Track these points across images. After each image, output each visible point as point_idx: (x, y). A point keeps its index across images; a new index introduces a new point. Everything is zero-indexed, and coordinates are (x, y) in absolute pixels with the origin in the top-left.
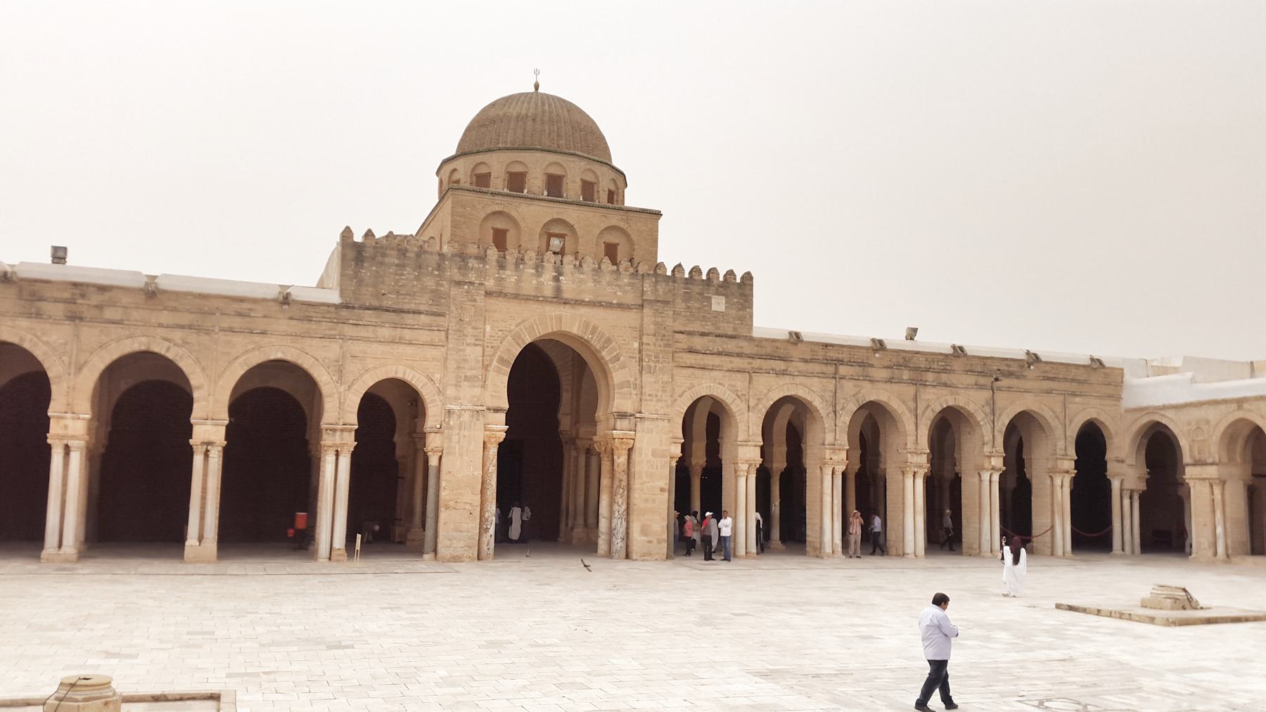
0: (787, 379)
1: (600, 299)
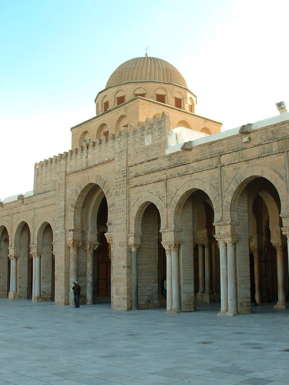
0: (187, 178)
1: (101, 160)
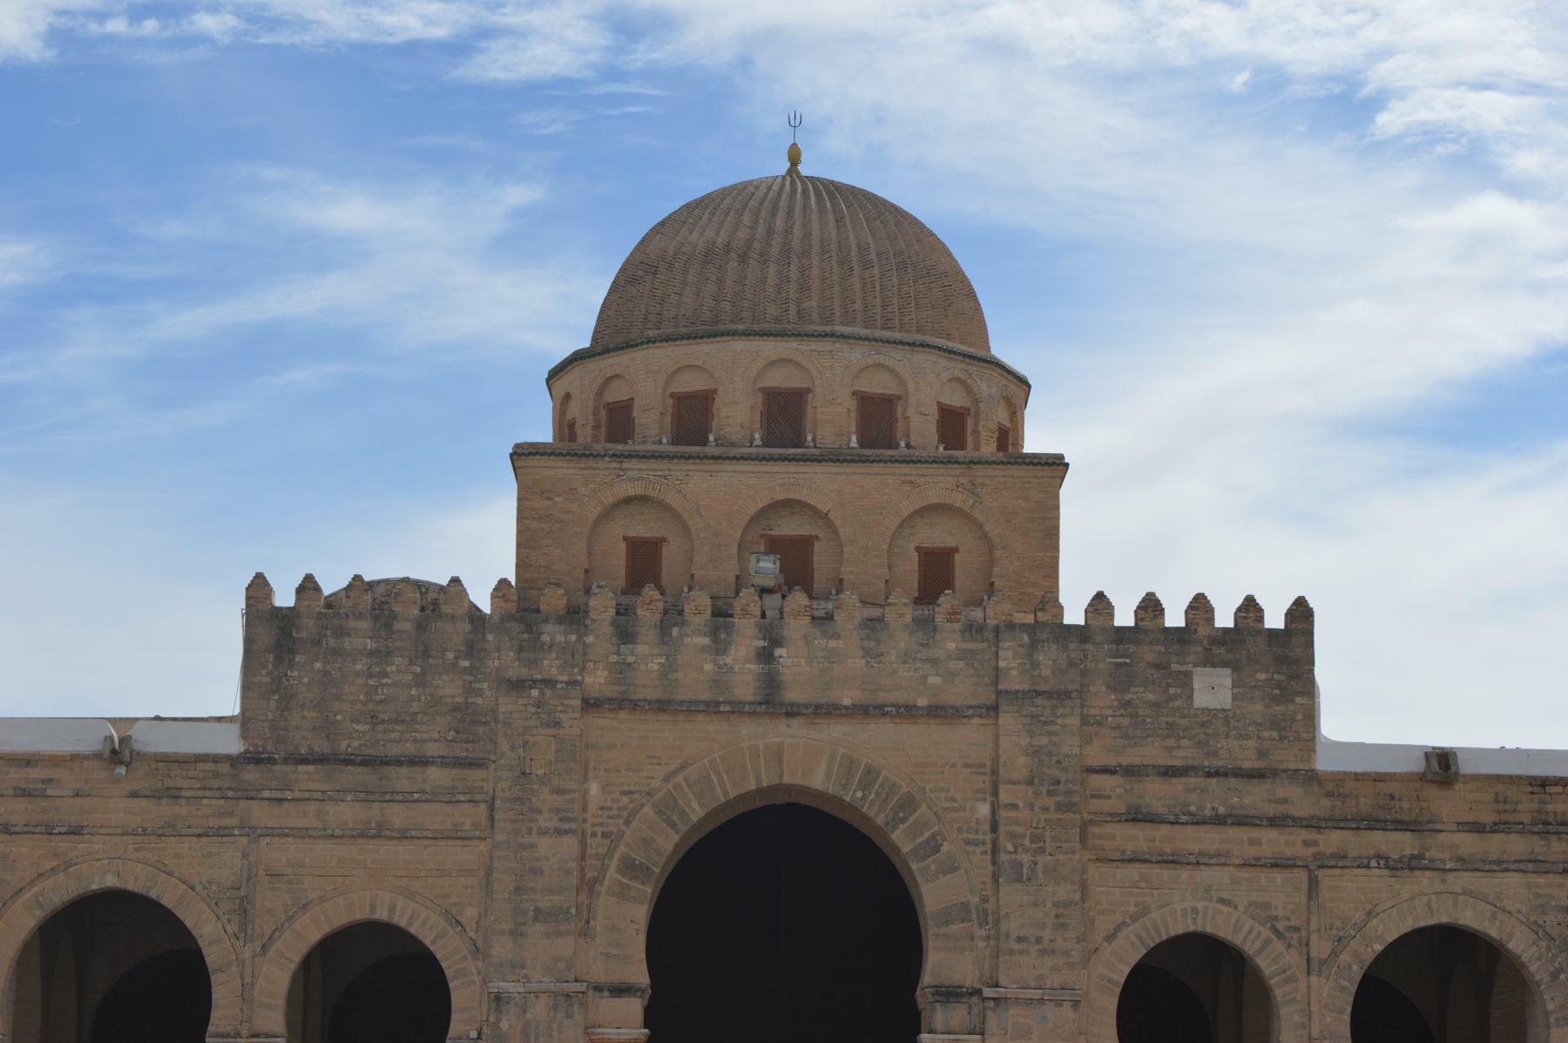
0: (1425, 880)
1: (883, 697)
